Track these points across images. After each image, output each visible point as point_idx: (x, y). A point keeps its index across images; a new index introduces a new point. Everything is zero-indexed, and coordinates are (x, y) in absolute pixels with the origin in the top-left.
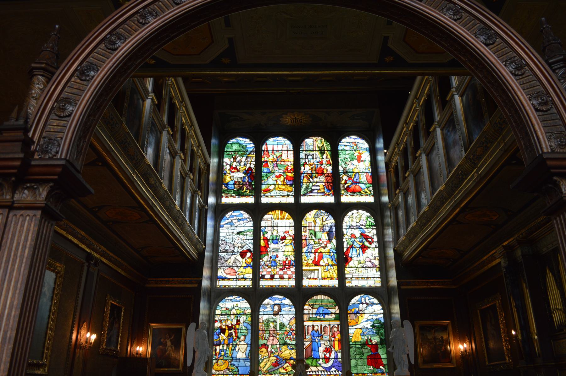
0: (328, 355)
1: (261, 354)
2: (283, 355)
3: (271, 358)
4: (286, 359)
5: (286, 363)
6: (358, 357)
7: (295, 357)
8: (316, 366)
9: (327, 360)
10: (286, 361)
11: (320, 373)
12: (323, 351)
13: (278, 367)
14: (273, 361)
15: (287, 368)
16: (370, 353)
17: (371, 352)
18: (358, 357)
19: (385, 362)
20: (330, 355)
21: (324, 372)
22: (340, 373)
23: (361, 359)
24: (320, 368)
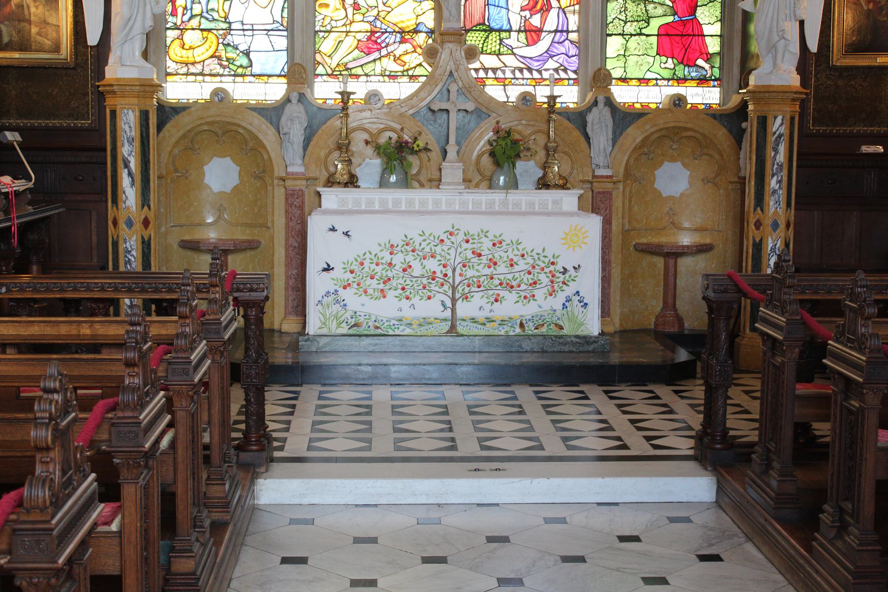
0: (536, 21)
1: (323, 11)
2: (391, 18)
3: (355, 27)
4: (402, 32)
5: (403, 41)
6: (630, 28)
7: (431, 24)
8: (499, 54)
9: (533, 34)
10: (404, 36)
11: (509, 75)
12: (523, 9)
13: (376, 55)
14: (360, 36)
15: (405, 58)
16: (670, 19)
17: (675, 13)
18: (630, 28)
19: (713, 46)
20: (543, 21)
21: (521, 70)
22: (573, 76)
23: (640, 34)
24: (510, 61)
